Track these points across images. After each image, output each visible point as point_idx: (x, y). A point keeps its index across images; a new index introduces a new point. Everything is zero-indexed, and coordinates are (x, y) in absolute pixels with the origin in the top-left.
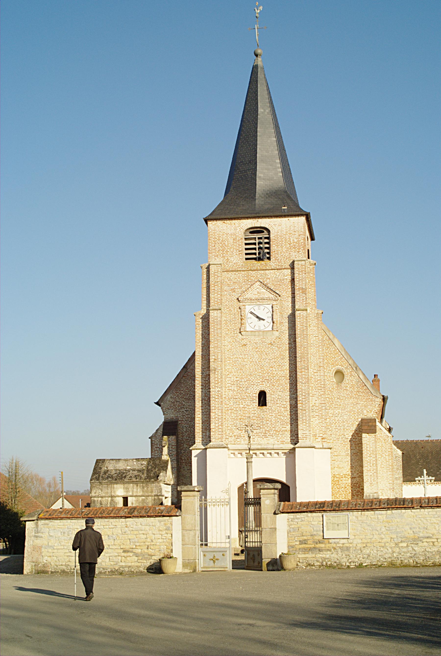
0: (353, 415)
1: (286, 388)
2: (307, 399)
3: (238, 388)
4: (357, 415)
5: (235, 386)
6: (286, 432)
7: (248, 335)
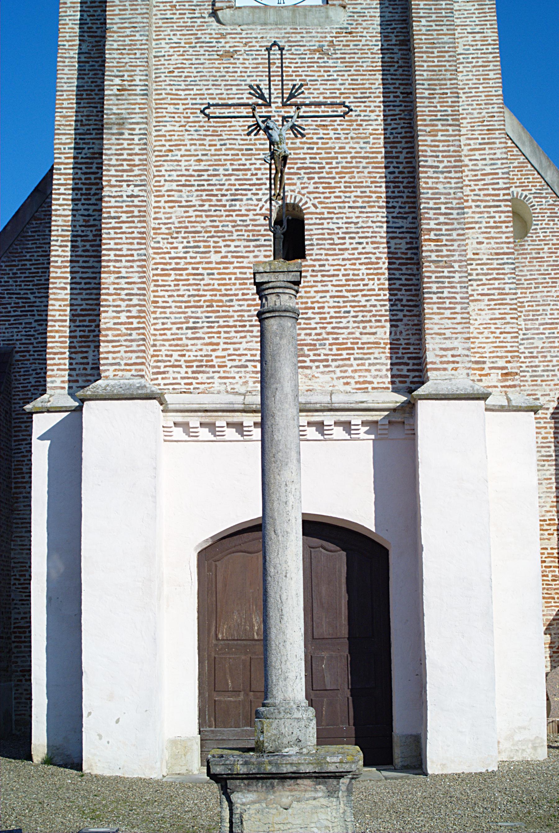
1: (374, 195)
2: (456, 226)
3: (204, 198)
5: (193, 189)
6: (377, 351)
7: (239, 21)
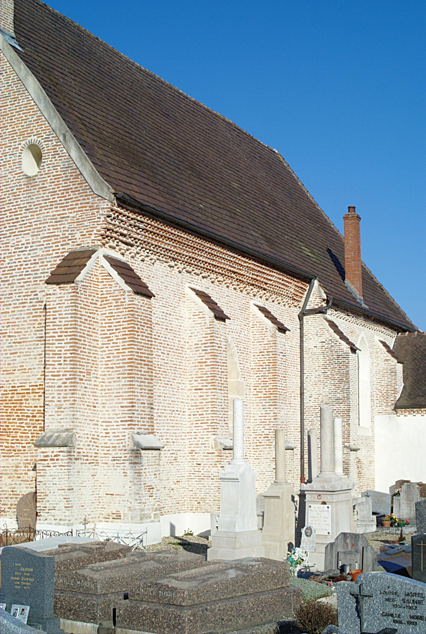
0: (54, 245)
4: (62, 245)
